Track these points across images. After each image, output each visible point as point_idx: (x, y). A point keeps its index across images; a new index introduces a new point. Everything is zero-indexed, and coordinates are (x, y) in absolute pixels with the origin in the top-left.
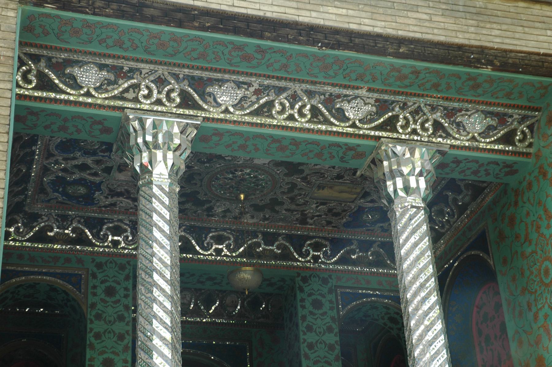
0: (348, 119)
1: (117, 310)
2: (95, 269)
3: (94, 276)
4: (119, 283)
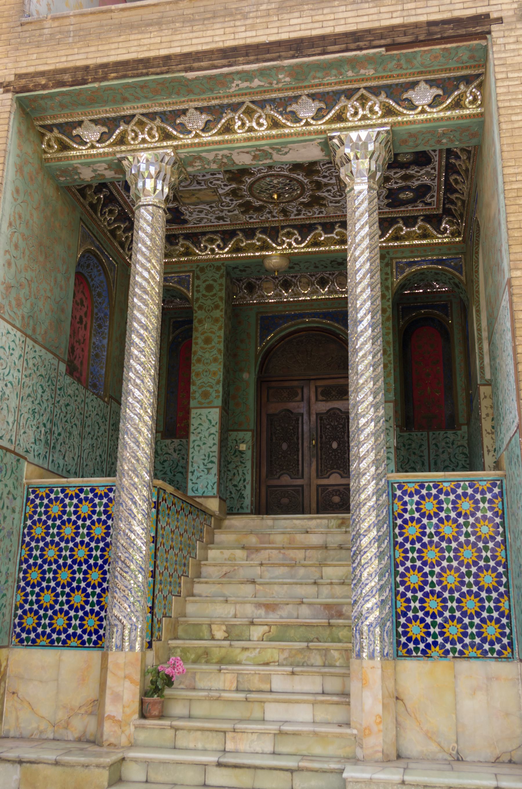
0: (86, 143)
2: (199, 273)
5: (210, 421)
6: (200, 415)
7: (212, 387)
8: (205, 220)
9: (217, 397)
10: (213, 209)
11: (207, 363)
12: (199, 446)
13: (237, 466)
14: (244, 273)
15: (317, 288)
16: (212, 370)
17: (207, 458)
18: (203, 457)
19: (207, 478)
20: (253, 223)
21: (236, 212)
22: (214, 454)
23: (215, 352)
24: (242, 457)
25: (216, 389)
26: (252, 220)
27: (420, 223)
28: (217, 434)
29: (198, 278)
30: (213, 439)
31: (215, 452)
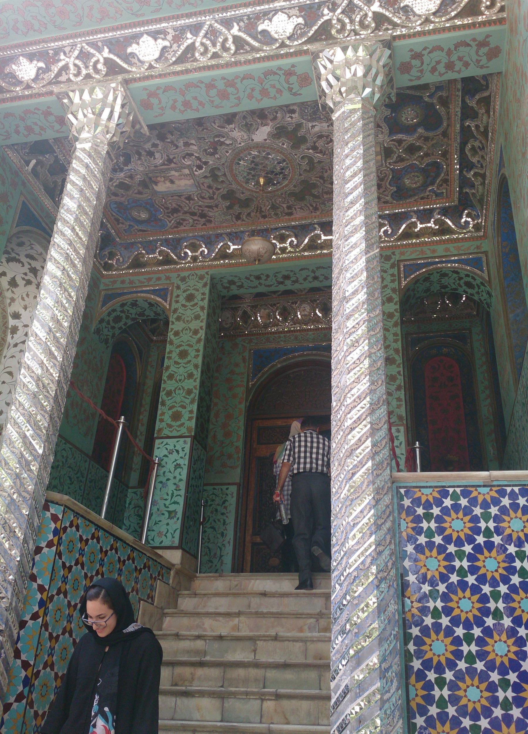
1: (195, 311)
2: (179, 283)
3: (178, 287)
4: (198, 290)
6: (167, 444)
17: (170, 497)
22: (179, 493)
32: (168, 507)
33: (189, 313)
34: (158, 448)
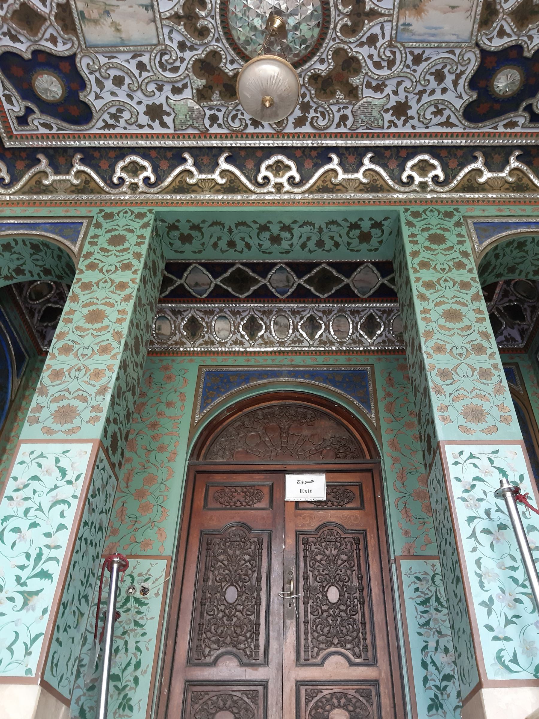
2: (101, 220)
5: (63, 472)
6: (42, 456)
7: (84, 399)
8: (126, 115)
9: (94, 420)
10: (145, 74)
11: (83, 355)
12: (16, 530)
13: (124, 633)
14: (187, 247)
15: (301, 335)
16: (92, 368)
18: (23, 561)
19: (16, 623)
20: (216, 136)
21: (188, 93)
22: (54, 553)
23: (109, 336)
24: (139, 612)
25: (94, 403)
26: (215, 130)
27: (514, 163)
28: (75, 503)
29: (98, 225)
30: (62, 515)
31: (57, 547)
32: (25, 584)
33: (113, 260)
34: (22, 463)
